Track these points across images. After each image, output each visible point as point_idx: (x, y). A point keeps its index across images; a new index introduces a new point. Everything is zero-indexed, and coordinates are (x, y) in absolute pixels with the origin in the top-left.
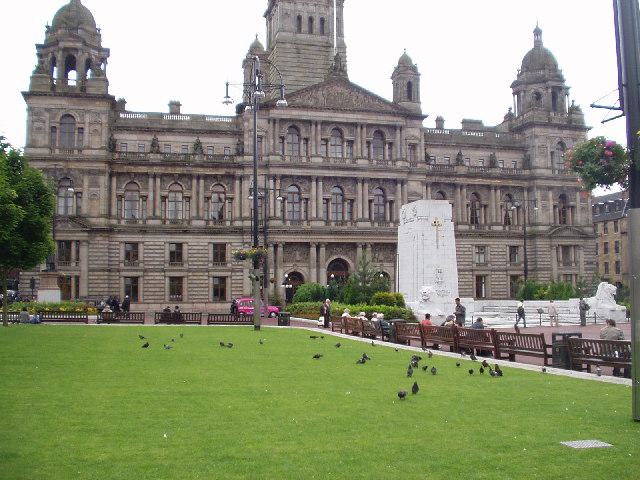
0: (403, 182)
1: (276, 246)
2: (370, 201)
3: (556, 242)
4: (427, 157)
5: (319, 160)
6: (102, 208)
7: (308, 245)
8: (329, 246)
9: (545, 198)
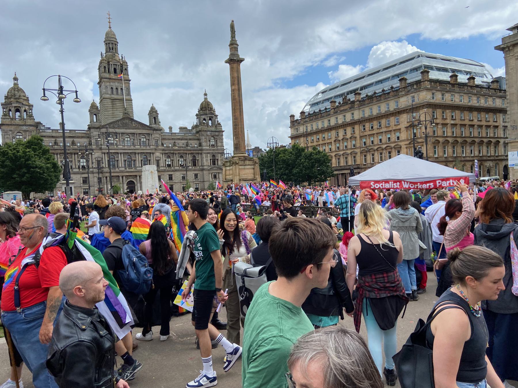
0: (153, 154)
1: (106, 177)
2: (141, 160)
3: (211, 172)
4: (163, 144)
5: (121, 147)
7: (119, 176)
8: (126, 176)
9: (207, 157)
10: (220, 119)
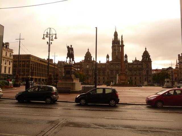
6: (91, 74)
10: (151, 57)
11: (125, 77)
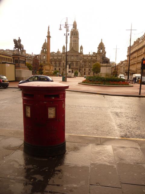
11: (49, 68)
